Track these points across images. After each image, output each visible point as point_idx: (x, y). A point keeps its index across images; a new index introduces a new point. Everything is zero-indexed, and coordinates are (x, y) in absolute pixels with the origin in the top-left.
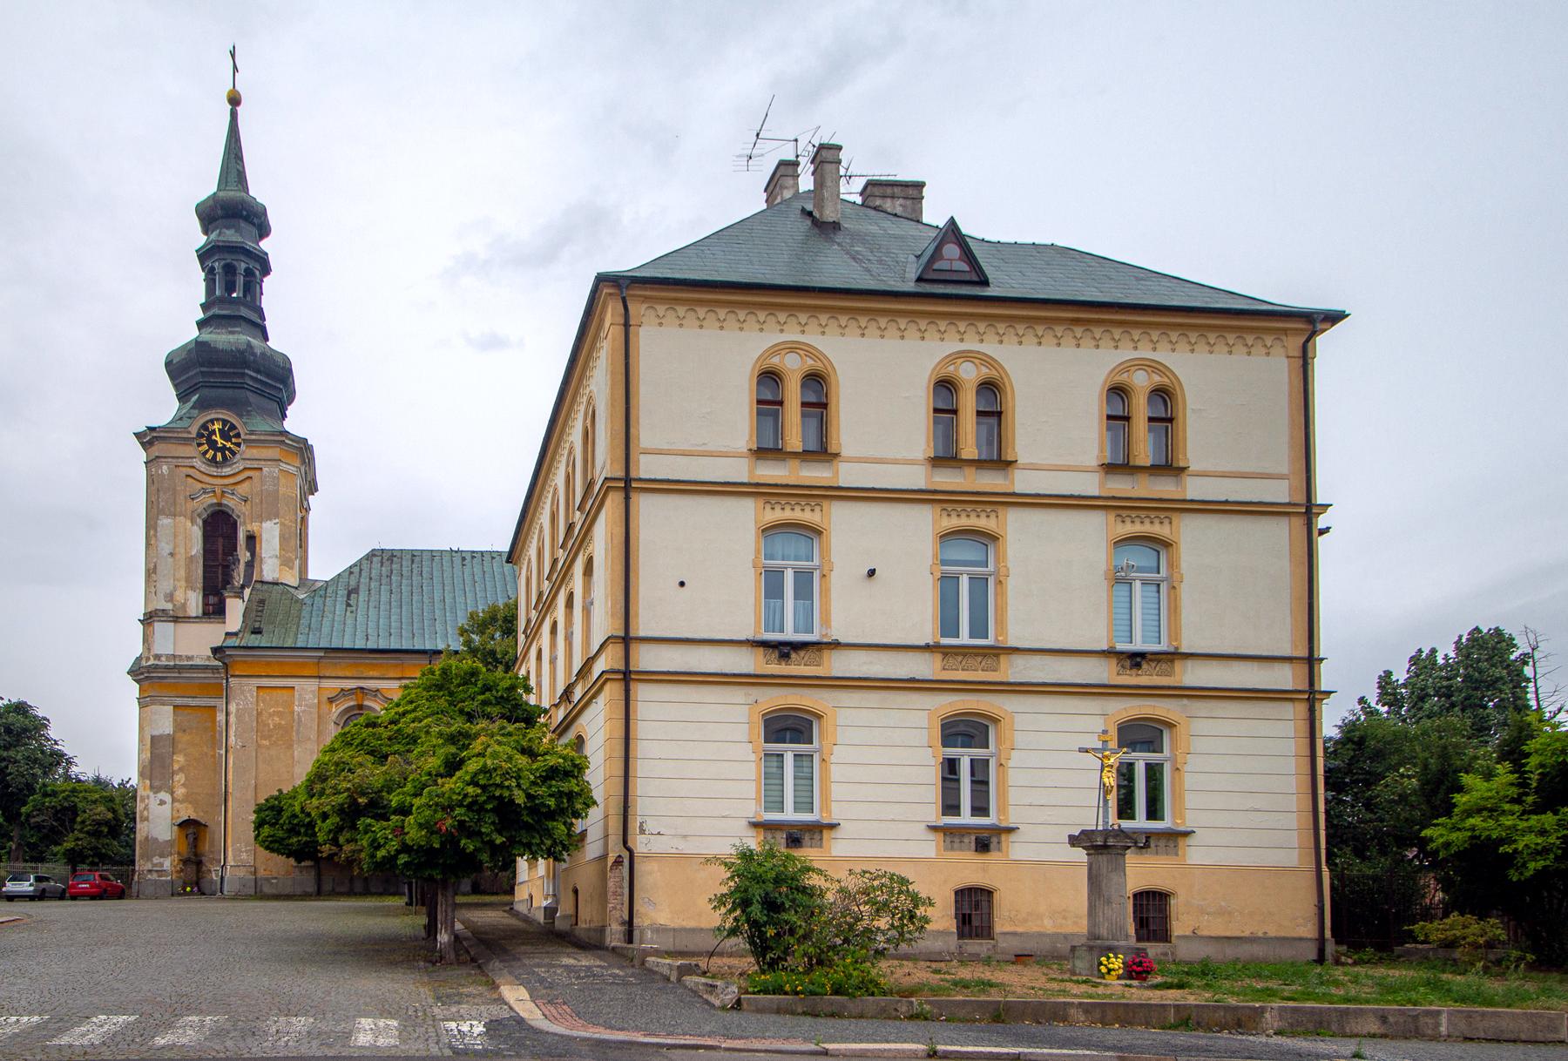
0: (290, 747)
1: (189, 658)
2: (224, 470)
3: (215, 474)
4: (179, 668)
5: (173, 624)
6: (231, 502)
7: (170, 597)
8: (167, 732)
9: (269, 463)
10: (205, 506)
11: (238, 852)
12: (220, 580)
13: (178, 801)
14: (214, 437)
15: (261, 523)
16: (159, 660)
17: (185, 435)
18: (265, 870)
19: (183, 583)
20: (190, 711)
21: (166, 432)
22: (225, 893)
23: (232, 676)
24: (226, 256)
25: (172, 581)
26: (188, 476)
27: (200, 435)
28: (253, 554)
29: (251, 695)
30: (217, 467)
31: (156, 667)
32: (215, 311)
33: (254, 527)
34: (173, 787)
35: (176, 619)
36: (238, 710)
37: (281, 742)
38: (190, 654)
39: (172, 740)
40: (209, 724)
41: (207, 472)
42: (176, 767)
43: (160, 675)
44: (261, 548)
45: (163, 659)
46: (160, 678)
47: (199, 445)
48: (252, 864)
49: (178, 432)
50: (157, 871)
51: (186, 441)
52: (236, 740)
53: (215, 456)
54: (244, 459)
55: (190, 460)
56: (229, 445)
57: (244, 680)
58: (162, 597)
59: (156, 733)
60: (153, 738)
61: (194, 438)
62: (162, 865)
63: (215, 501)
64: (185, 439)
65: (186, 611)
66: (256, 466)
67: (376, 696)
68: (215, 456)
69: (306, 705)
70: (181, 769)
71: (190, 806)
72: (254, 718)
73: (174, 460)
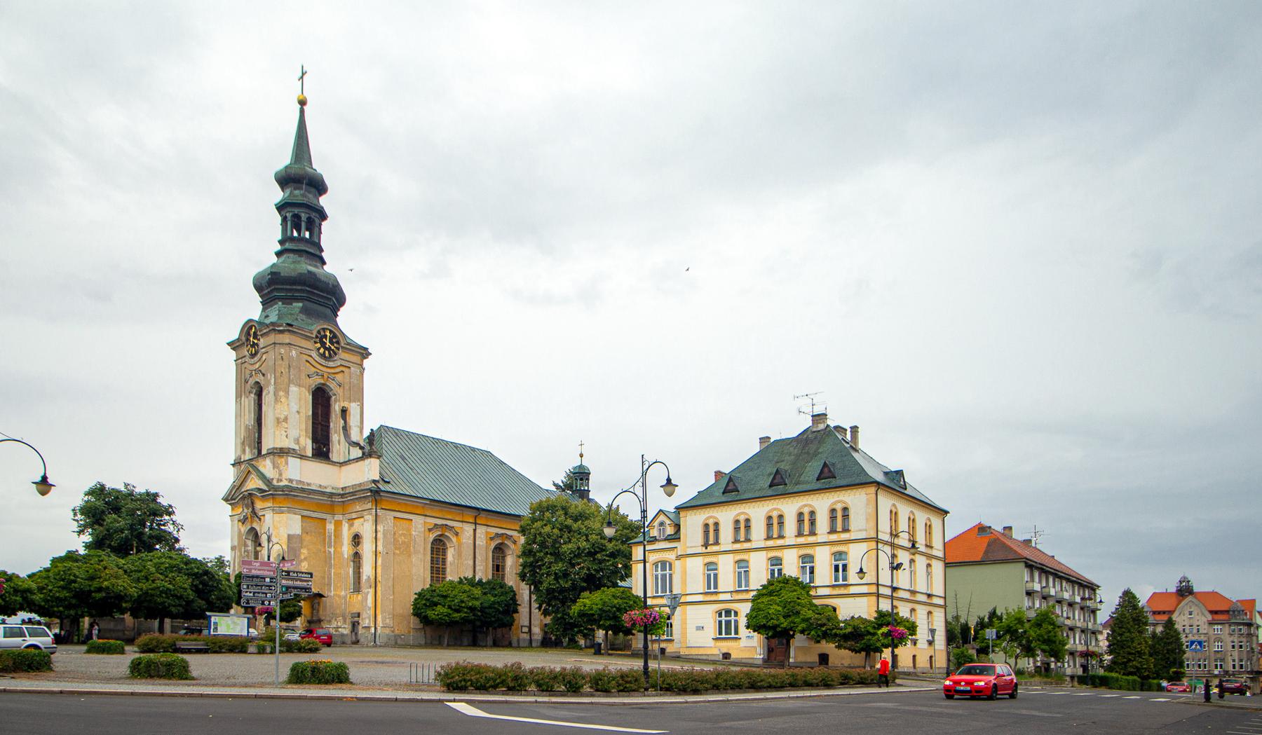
1: (309, 484)
2: (330, 363)
4: (303, 490)
5: (299, 460)
6: (332, 385)
7: (297, 441)
12: (320, 434)
17: (309, 334)
19: (304, 433)
24: (310, 212)
26: (307, 361)
27: (317, 337)
28: (345, 422)
29: (390, 521)
30: (326, 360)
32: (287, 245)
33: (346, 404)
35: (302, 457)
36: (384, 530)
38: (309, 482)
39: (300, 538)
42: (302, 557)
44: (350, 419)
45: (294, 483)
46: (295, 496)
47: (316, 343)
51: (307, 338)
56: (333, 347)
59: (291, 533)
60: (289, 535)
63: (323, 382)
64: (309, 337)
68: (324, 352)
70: (305, 559)
72: (392, 536)
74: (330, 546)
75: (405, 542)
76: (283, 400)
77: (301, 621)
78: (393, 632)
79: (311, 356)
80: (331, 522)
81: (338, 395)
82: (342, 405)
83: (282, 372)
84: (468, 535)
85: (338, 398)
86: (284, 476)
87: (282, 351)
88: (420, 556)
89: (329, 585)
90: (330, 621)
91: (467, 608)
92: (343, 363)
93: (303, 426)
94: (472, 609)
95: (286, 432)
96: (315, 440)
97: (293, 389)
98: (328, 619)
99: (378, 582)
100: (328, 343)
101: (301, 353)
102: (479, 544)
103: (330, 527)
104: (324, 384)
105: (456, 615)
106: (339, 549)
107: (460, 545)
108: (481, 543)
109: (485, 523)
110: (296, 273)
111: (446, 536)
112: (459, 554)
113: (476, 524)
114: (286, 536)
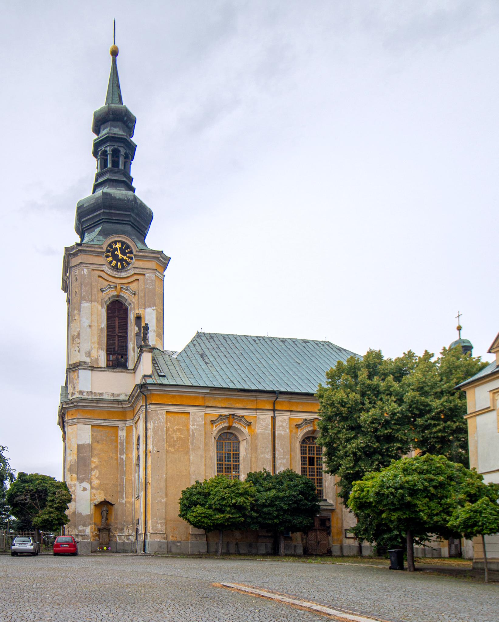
0: (187, 453)
1: (101, 394)
2: (123, 274)
3: (117, 276)
5: (90, 371)
6: (125, 295)
7: (89, 354)
8: (87, 443)
10: (110, 296)
11: (155, 524)
13: (94, 488)
14: (116, 253)
15: (145, 309)
16: (82, 394)
17: (99, 250)
18: (172, 536)
20: (101, 429)
21: (87, 247)
22: (147, 551)
23: (151, 404)
25: (90, 343)
26: (99, 276)
27: (108, 251)
30: (118, 272)
31: (82, 400)
33: (141, 311)
34: (91, 479)
35: (93, 369)
36: (154, 427)
37: (181, 450)
38: (101, 392)
39: (90, 447)
40: (114, 438)
41: (111, 275)
42: (93, 466)
43: (84, 404)
45: (85, 394)
47: (107, 257)
48: (165, 532)
49: (95, 248)
50: (81, 535)
51: (99, 254)
52: (153, 447)
53: (117, 265)
54: (134, 268)
55: (101, 266)
57: (158, 407)
58: (84, 353)
60: (79, 446)
61: (104, 252)
62: (84, 531)
63: (116, 293)
64: (98, 252)
65: (98, 364)
66: (141, 273)
67: (240, 421)
68: (117, 265)
69: (197, 425)
70: (96, 467)
71: (102, 492)
73: (92, 266)
74: (122, 454)
75: (180, 437)
77: (91, 528)
78: (166, 538)
79: (103, 271)
80: (123, 429)
81: (132, 304)
82: (137, 312)
84: (264, 424)
85: (132, 307)
88: (201, 452)
89: (122, 492)
90: (122, 529)
91: (229, 506)
92: (137, 271)
93: (96, 339)
94: (239, 508)
96: (110, 351)
98: (120, 526)
99: (148, 484)
100: (120, 255)
102: (280, 435)
103: (122, 434)
104: (118, 296)
105: (220, 516)
106: (130, 456)
107: (254, 436)
108: (283, 433)
109: (288, 409)
111: (236, 428)
112: (253, 448)
113: (274, 410)
114: (76, 446)
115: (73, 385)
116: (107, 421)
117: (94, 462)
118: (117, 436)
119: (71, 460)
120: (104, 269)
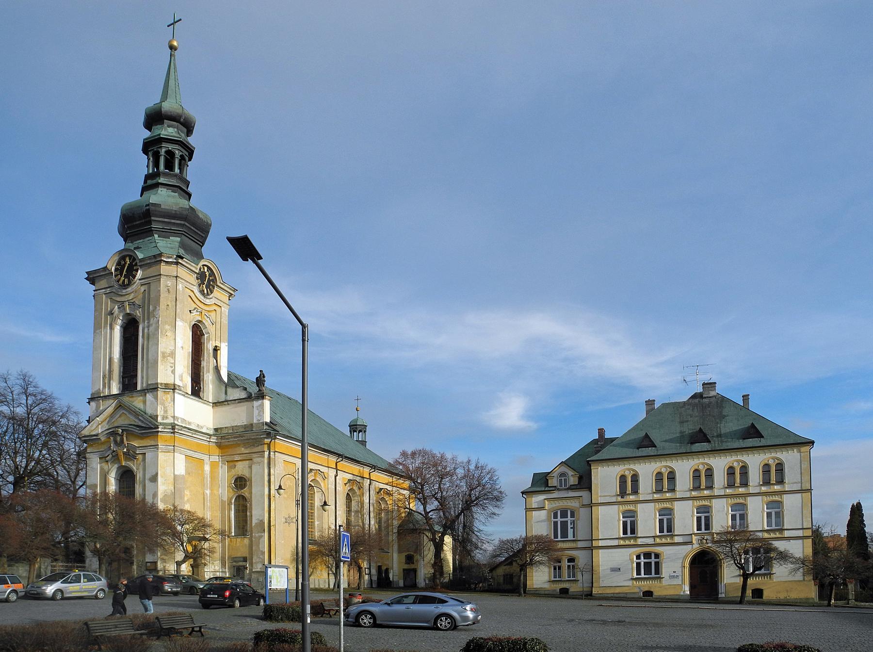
1: (190, 423)
3: (203, 301)
6: (207, 322)
8: (182, 474)
9: (225, 305)
38: (190, 421)
40: (200, 472)
42: (186, 499)
45: (179, 421)
76: (169, 334)
83: (168, 305)
86: (170, 413)
87: (169, 283)
95: (172, 367)
97: (179, 323)
101: (186, 287)
104: (200, 321)
110: (178, 207)
115: (164, 408)
116: (196, 453)
117: (187, 495)
118: (203, 470)
119: (165, 490)
120: (194, 290)
